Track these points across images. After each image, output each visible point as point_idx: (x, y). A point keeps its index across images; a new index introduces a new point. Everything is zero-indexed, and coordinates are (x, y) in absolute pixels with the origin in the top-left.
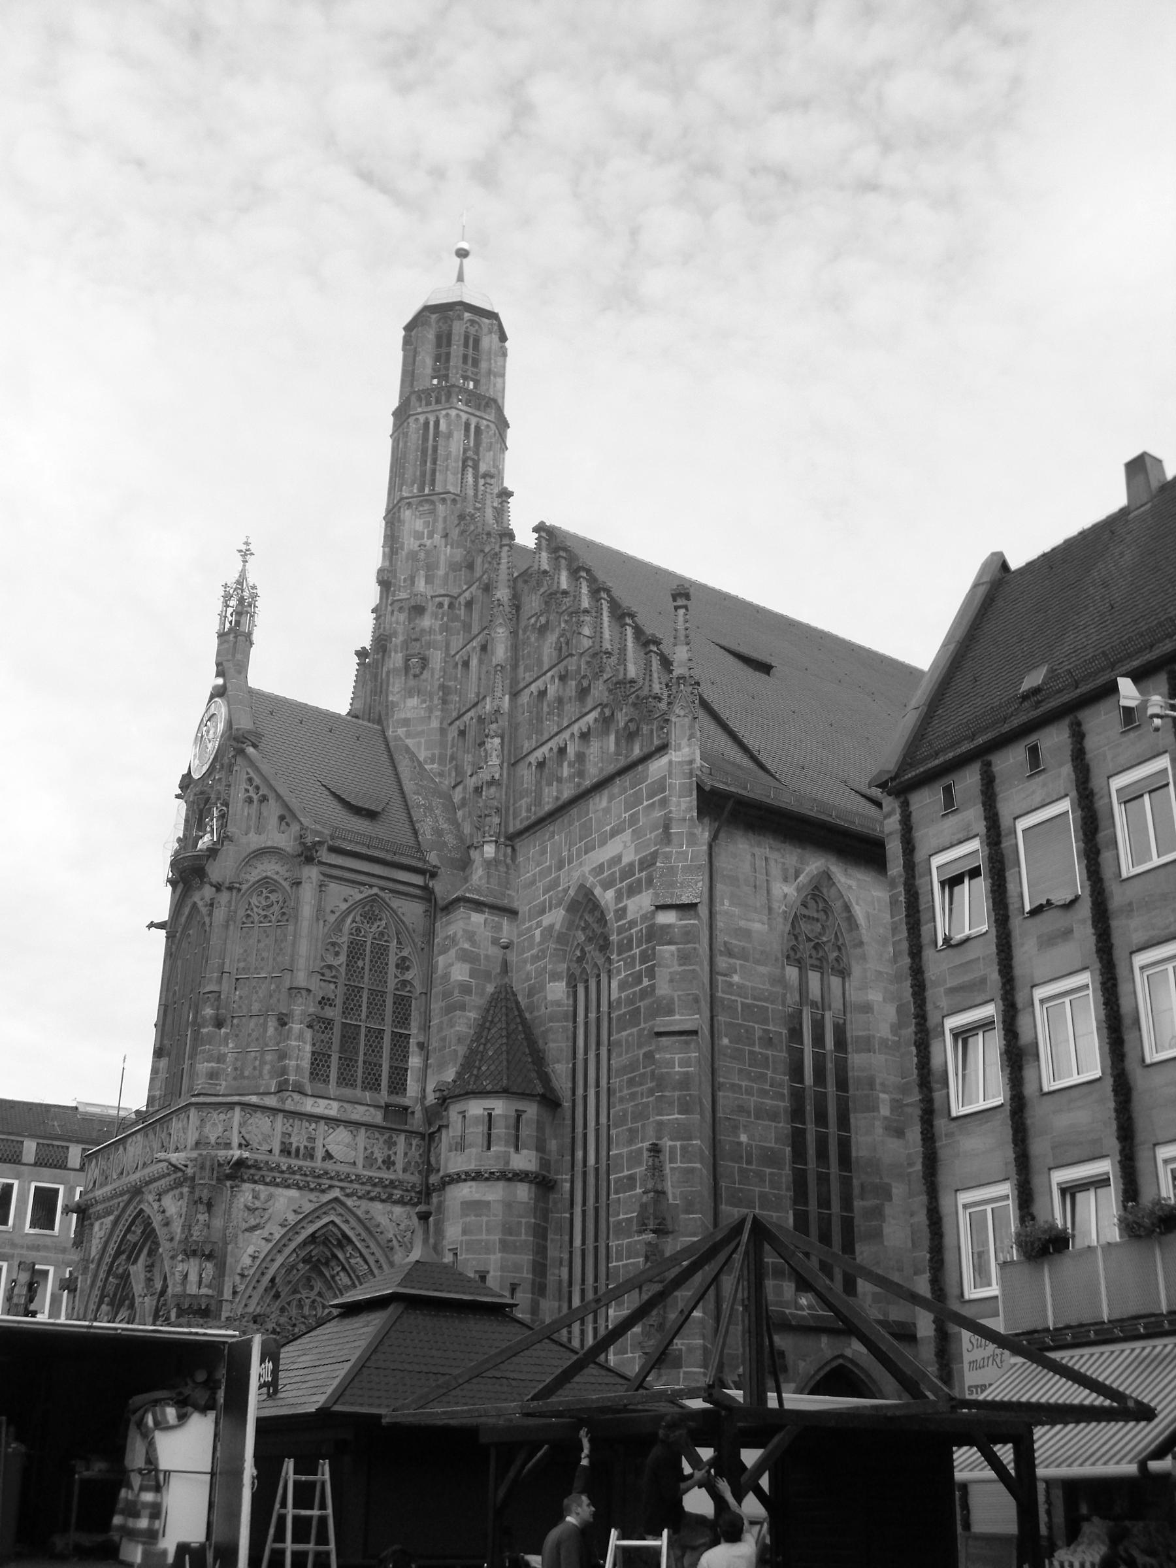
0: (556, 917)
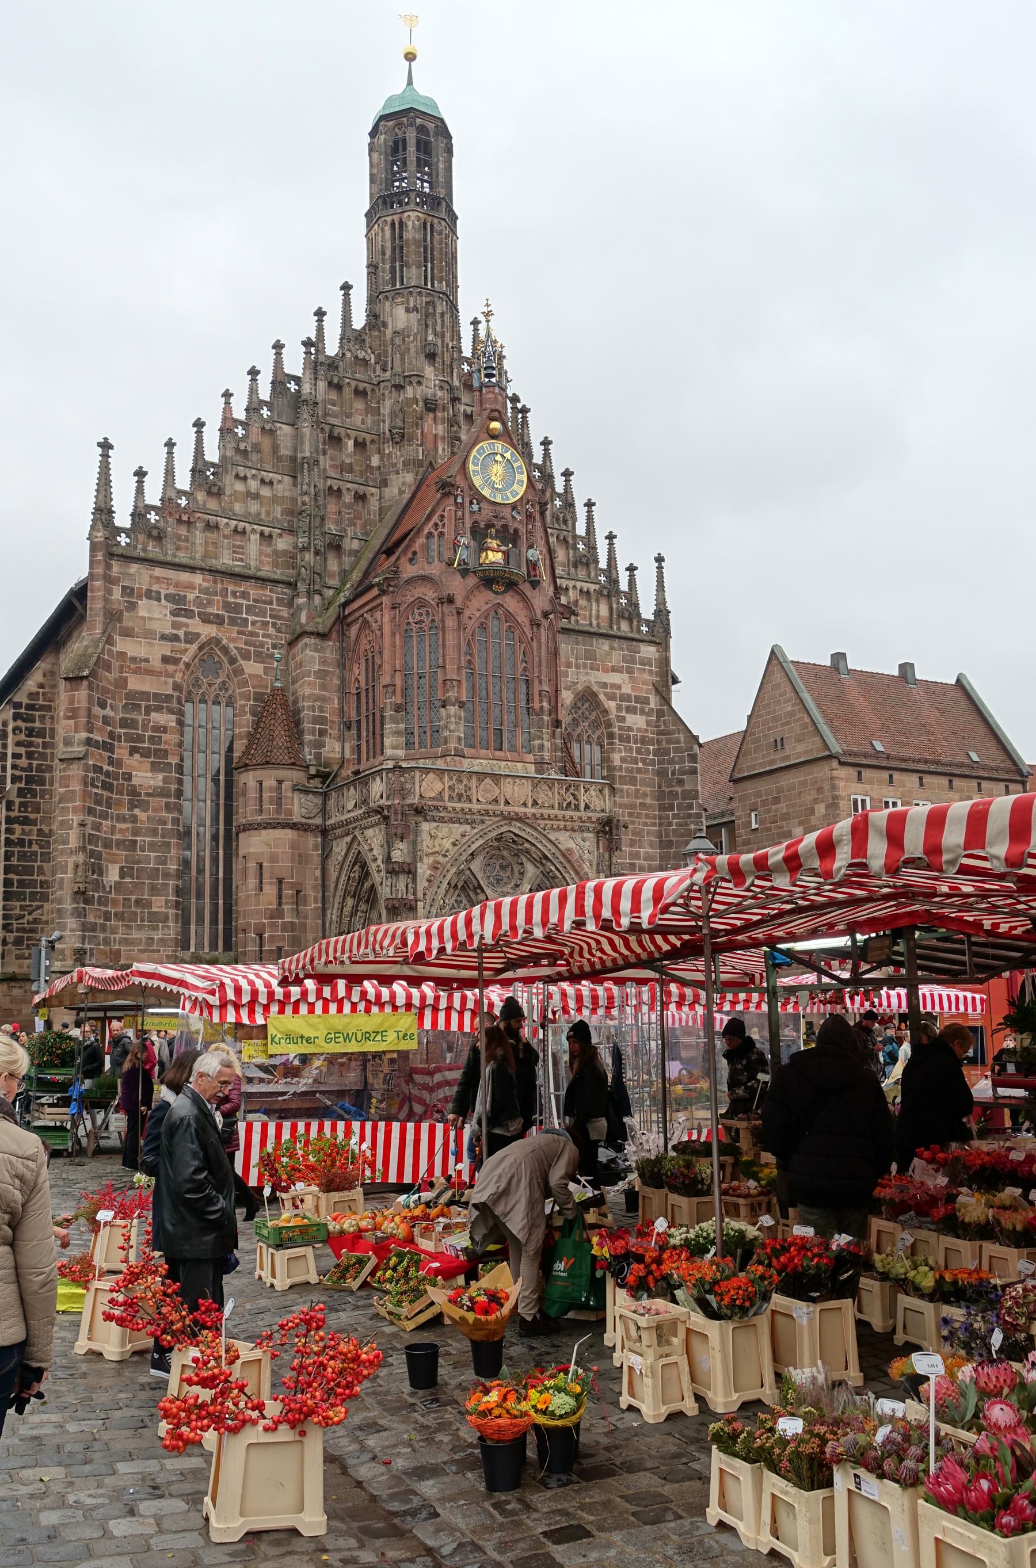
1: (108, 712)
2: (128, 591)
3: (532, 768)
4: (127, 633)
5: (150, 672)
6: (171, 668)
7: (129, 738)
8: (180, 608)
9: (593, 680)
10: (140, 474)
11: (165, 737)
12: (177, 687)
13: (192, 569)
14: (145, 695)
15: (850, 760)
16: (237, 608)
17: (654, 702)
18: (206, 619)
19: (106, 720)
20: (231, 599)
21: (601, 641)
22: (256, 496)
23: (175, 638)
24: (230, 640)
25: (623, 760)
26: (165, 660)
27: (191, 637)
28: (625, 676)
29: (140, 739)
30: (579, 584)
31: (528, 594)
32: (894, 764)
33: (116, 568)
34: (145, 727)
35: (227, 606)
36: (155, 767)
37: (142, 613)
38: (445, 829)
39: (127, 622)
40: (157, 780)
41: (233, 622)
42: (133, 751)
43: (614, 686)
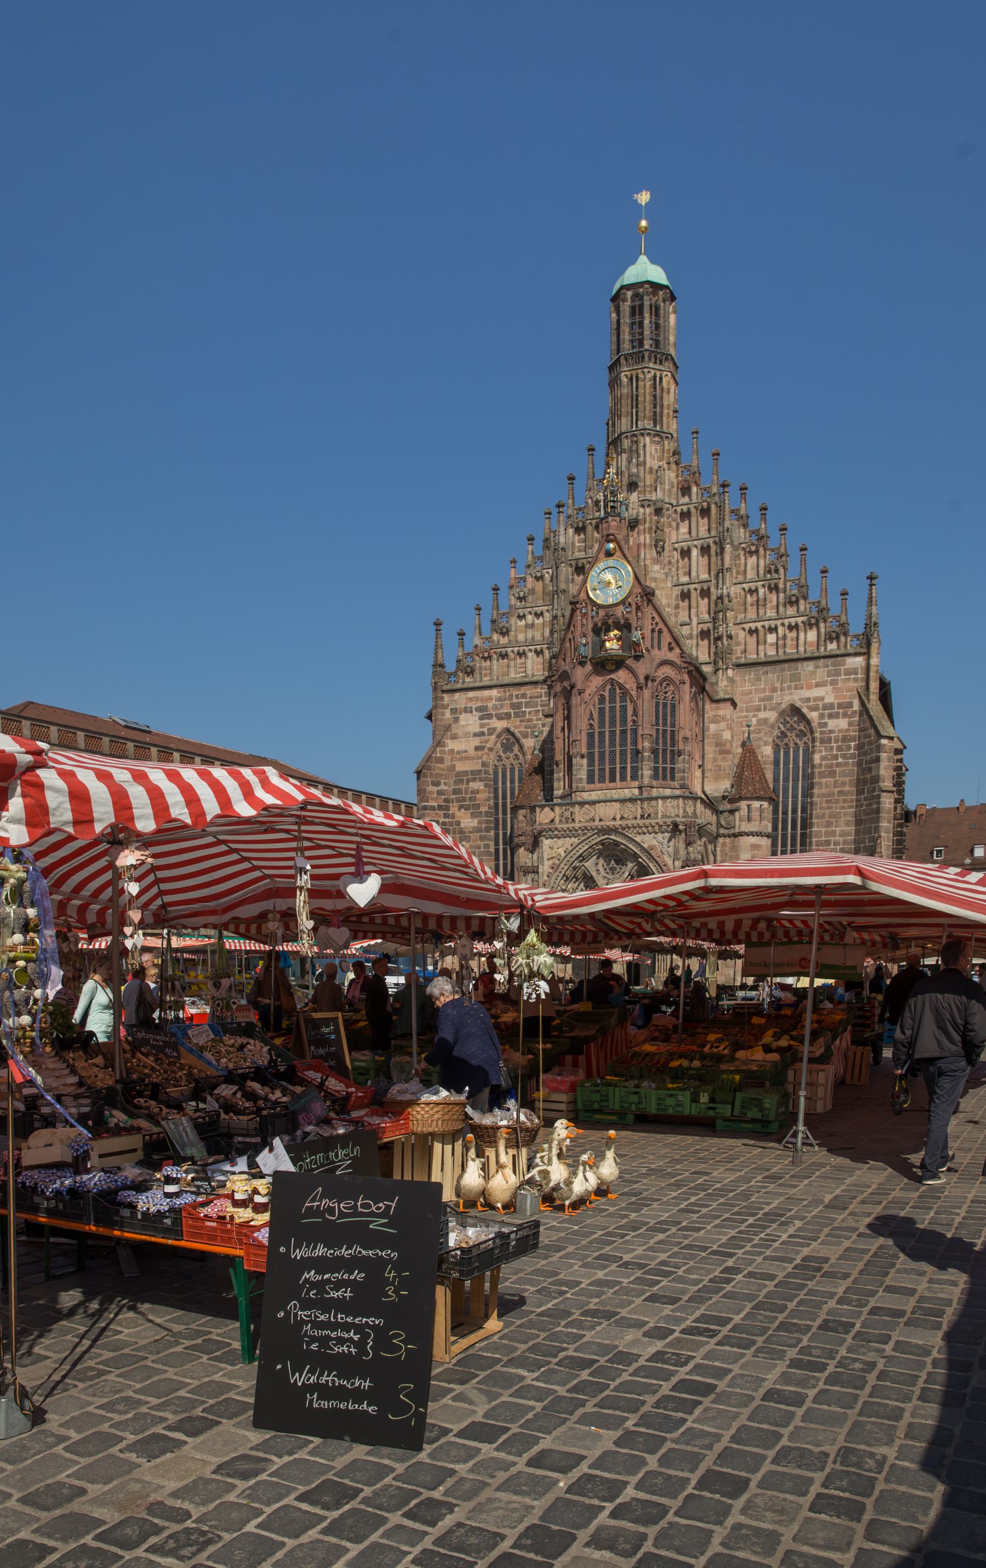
1: (442, 787)
2: (454, 711)
3: (636, 792)
4: (454, 737)
5: (468, 758)
6: (480, 753)
7: (458, 800)
8: (485, 714)
9: (796, 697)
10: (462, 634)
11: (478, 796)
12: (484, 764)
13: (490, 687)
14: (466, 773)
18: (500, 717)
19: (440, 793)
20: (515, 701)
21: (805, 664)
23: (482, 734)
24: (516, 727)
26: (477, 748)
27: (491, 731)
29: (464, 800)
30: (786, 622)
31: (634, 666)
33: (446, 697)
34: (466, 793)
35: (513, 706)
36: (473, 816)
37: (462, 722)
39: (454, 731)
40: (474, 823)
41: (517, 715)
42: (460, 807)
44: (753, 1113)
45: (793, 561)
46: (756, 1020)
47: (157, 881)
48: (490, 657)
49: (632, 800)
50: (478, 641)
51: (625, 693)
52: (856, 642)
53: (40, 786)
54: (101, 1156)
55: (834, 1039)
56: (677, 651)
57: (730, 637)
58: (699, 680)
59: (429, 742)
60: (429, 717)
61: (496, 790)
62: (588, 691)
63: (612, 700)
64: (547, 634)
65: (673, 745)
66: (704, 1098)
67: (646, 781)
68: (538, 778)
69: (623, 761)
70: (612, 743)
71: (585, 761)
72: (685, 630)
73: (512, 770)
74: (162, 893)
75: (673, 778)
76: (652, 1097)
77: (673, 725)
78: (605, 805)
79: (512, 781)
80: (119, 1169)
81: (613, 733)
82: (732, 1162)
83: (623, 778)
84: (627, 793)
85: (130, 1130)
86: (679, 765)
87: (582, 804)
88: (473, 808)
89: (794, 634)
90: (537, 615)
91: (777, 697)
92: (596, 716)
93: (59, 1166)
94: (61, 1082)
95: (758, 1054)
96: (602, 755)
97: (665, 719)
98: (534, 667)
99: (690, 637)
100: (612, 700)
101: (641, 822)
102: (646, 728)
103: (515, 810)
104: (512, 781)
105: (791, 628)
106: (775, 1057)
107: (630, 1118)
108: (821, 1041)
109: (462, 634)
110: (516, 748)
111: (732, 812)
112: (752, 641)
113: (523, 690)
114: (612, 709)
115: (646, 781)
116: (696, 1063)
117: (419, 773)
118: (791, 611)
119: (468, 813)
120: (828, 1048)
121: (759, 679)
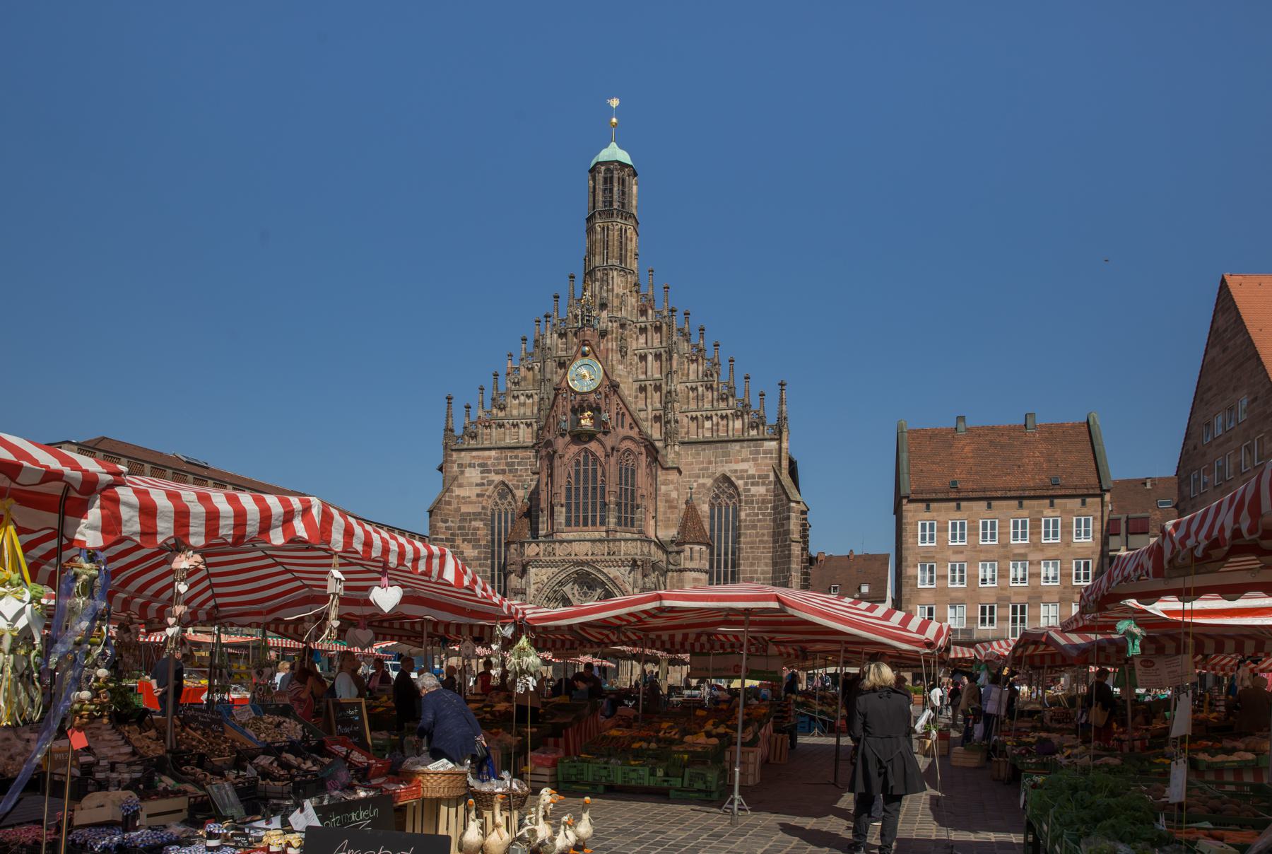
0: (709, 482)
1: (450, 524)
2: (460, 466)
3: (604, 534)
4: (460, 486)
5: (471, 503)
7: (462, 535)
8: (485, 469)
10: (468, 407)
12: (483, 508)
13: (489, 449)
15: (920, 496)
16: (512, 464)
17: (772, 477)
18: (497, 473)
19: (447, 528)
22: (524, 404)
23: (483, 484)
25: (747, 515)
26: (478, 495)
27: (490, 483)
28: (751, 463)
32: (962, 495)
33: (455, 455)
35: (507, 464)
37: (467, 475)
38: (544, 570)
41: (510, 471)
42: (464, 540)
43: (742, 471)
44: (699, 785)
45: (725, 368)
46: (699, 713)
47: (212, 586)
48: (490, 426)
49: (600, 541)
50: (481, 413)
51: (596, 459)
52: (771, 431)
53: (116, 501)
54: (149, 816)
55: (760, 728)
56: (636, 429)
57: (677, 422)
58: (653, 453)
59: (440, 489)
60: (441, 469)
61: (493, 529)
62: (567, 456)
63: (586, 464)
64: (535, 411)
65: (633, 500)
66: (660, 773)
67: (612, 526)
68: (527, 520)
69: (594, 510)
70: (586, 496)
71: (564, 509)
72: (642, 415)
73: (506, 514)
74: (215, 596)
75: (632, 525)
76: (618, 772)
77: (633, 485)
78: (580, 544)
79: (506, 522)
80: (165, 827)
81: (586, 489)
82: (682, 823)
83: (594, 524)
84: (596, 535)
85: (176, 793)
86: (637, 516)
87: (561, 542)
88: (475, 542)
89: (725, 422)
90: (528, 397)
91: (712, 468)
92: (573, 475)
93: (109, 825)
94: (116, 751)
95: (702, 739)
96: (577, 505)
97: (626, 481)
98: (525, 435)
99: (647, 420)
100: (586, 464)
101: (608, 558)
102: (612, 486)
103: (508, 544)
104: (506, 522)
105: (722, 417)
106: (715, 741)
107: (601, 789)
108: (750, 728)
109: (468, 407)
110: (510, 497)
111: (678, 553)
112: (693, 425)
113: (516, 452)
114: (586, 471)
115: (612, 526)
116: (653, 745)
117: (431, 512)
118: (723, 405)
119: (470, 545)
120: (756, 735)
121: (698, 454)
